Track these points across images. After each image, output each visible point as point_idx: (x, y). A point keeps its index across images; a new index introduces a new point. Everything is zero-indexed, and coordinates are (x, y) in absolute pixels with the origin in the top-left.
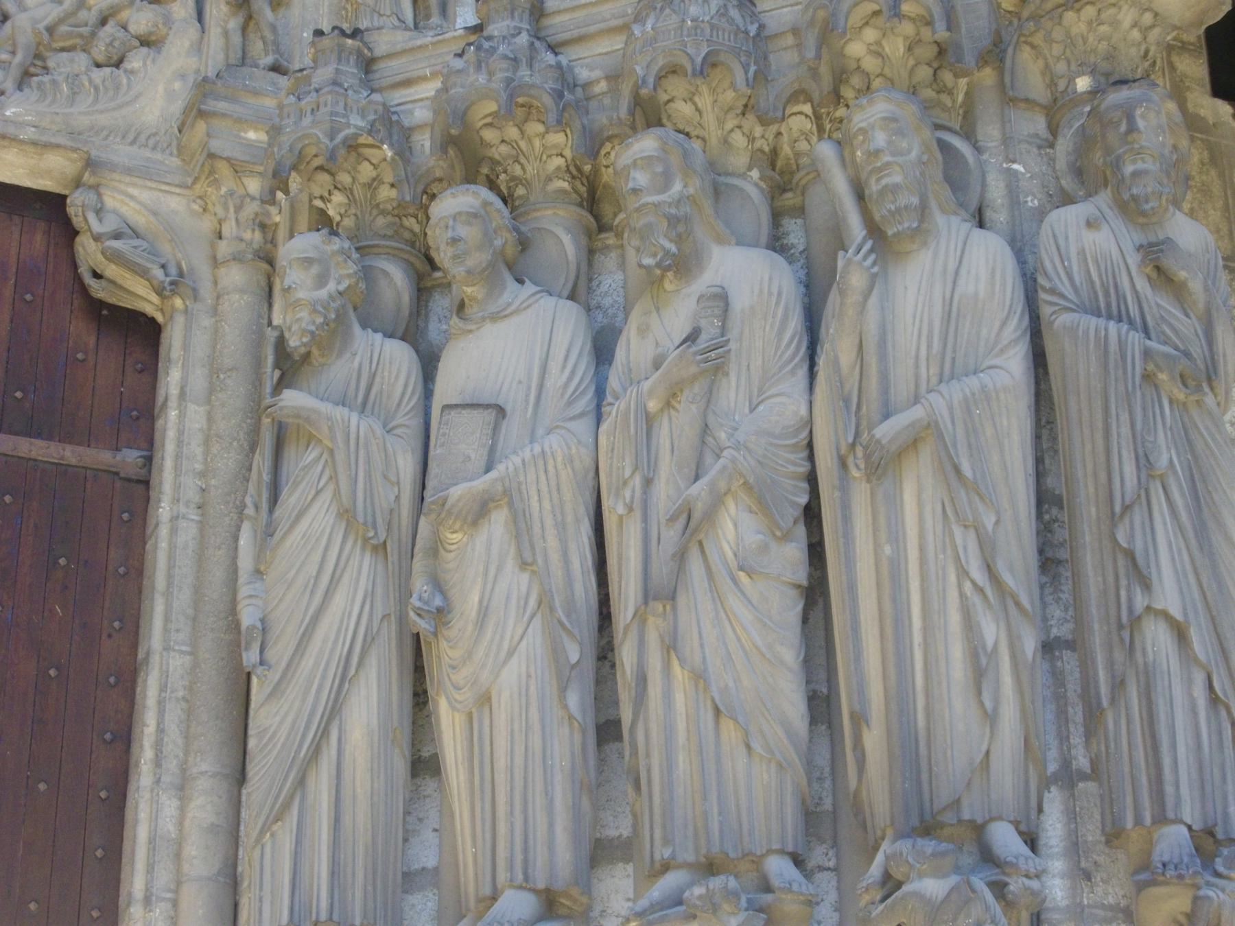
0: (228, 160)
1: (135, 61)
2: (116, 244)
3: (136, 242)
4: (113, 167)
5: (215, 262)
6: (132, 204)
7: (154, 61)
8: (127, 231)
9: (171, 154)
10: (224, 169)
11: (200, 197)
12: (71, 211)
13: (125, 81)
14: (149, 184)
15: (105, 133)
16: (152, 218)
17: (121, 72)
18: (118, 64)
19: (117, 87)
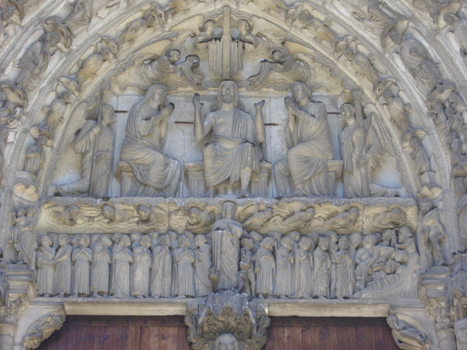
0: (434, 298)
1: (399, 271)
2: (405, 331)
3: (411, 329)
4: (399, 307)
5: (437, 331)
6: (407, 317)
7: (405, 269)
8: (407, 326)
9: (416, 298)
10: (433, 301)
11: (428, 310)
12: (389, 323)
13: (397, 277)
14: (411, 309)
15: (394, 296)
16: (414, 320)
17: (396, 275)
18: (394, 273)
19: (396, 281)
